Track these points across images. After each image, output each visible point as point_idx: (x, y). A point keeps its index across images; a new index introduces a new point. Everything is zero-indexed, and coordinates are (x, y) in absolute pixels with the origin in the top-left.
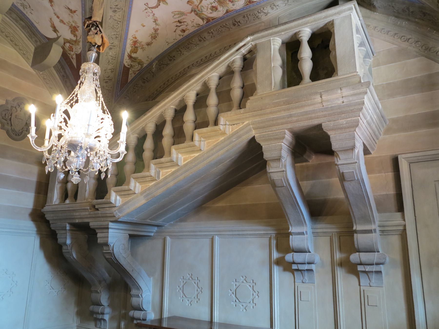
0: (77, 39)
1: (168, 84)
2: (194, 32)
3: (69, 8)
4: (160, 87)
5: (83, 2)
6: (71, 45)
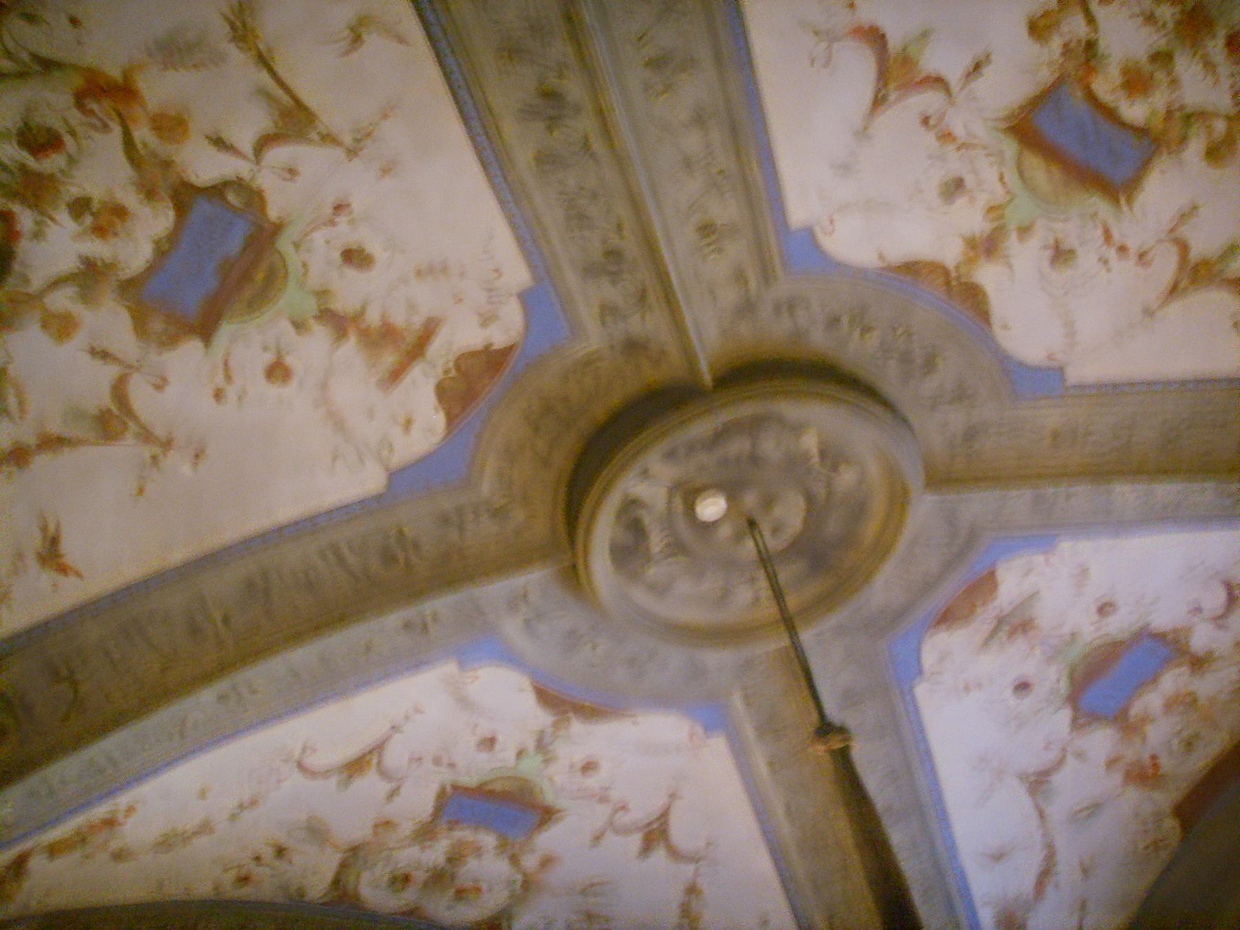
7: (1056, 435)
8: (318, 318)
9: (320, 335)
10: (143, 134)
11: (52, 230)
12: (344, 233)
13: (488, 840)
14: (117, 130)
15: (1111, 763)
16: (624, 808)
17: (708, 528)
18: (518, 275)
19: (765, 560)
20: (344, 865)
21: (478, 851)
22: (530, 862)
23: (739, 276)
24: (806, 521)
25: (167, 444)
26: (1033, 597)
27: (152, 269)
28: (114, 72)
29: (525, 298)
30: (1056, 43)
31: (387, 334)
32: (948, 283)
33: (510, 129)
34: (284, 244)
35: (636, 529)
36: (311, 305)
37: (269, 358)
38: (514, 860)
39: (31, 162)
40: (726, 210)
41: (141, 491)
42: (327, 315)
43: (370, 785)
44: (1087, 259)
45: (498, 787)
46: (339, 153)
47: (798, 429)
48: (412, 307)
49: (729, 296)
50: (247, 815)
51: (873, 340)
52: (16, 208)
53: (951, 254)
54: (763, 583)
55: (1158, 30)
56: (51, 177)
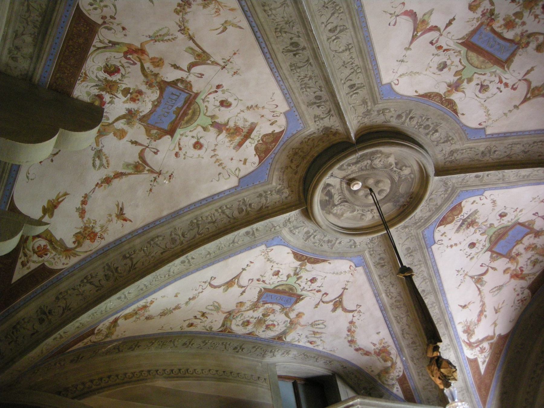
0: (76, 247)
1: (108, 382)
2: (200, 333)
3: (122, 209)
4: (92, 381)
5: (158, 222)
6: (49, 247)
7: (483, 153)
8: (211, 125)
9: (213, 131)
10: (147, 65)
11: (116, 100)
12: (220, 96)
13: (277, 307)
14: (139, 64)
15: (505, 272)
16: (326, 294)
17: (356, 192)
18: (284, 107)
19: (376, 203)
20: (226, 318)
21: (273, 311)
22: (292, 315)
23: (364, 102)
24: (391, 189)
25: (160, 173)
26: (476, 212)
27: (151, 112)
28: (138, 45)
29: (286, 114)
30: (479, 11)
31: (237, 130)
32: (441, 99)
33: (280, 56)
34: (199, 100)
35: (330, 195)
36: (209, 121)
37: (195, 140)
38: (287, 315)
39: (109, 78)
40: (359, 79)
41: (151, 190)
42: (215, 125)
43: (235, 290)
44: (493, 88)
45: (280, 288)
46: (219, 68)
47: (388, 156)
48: (245, 120)
49: (361, 110)
50: (192, 302)
51: (414, 122)
52: (103, 93)
53: (442, 89)
54: (376, 211)
55: (516, 5)
56: (115, 82)
